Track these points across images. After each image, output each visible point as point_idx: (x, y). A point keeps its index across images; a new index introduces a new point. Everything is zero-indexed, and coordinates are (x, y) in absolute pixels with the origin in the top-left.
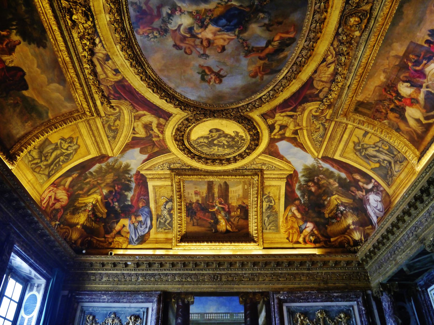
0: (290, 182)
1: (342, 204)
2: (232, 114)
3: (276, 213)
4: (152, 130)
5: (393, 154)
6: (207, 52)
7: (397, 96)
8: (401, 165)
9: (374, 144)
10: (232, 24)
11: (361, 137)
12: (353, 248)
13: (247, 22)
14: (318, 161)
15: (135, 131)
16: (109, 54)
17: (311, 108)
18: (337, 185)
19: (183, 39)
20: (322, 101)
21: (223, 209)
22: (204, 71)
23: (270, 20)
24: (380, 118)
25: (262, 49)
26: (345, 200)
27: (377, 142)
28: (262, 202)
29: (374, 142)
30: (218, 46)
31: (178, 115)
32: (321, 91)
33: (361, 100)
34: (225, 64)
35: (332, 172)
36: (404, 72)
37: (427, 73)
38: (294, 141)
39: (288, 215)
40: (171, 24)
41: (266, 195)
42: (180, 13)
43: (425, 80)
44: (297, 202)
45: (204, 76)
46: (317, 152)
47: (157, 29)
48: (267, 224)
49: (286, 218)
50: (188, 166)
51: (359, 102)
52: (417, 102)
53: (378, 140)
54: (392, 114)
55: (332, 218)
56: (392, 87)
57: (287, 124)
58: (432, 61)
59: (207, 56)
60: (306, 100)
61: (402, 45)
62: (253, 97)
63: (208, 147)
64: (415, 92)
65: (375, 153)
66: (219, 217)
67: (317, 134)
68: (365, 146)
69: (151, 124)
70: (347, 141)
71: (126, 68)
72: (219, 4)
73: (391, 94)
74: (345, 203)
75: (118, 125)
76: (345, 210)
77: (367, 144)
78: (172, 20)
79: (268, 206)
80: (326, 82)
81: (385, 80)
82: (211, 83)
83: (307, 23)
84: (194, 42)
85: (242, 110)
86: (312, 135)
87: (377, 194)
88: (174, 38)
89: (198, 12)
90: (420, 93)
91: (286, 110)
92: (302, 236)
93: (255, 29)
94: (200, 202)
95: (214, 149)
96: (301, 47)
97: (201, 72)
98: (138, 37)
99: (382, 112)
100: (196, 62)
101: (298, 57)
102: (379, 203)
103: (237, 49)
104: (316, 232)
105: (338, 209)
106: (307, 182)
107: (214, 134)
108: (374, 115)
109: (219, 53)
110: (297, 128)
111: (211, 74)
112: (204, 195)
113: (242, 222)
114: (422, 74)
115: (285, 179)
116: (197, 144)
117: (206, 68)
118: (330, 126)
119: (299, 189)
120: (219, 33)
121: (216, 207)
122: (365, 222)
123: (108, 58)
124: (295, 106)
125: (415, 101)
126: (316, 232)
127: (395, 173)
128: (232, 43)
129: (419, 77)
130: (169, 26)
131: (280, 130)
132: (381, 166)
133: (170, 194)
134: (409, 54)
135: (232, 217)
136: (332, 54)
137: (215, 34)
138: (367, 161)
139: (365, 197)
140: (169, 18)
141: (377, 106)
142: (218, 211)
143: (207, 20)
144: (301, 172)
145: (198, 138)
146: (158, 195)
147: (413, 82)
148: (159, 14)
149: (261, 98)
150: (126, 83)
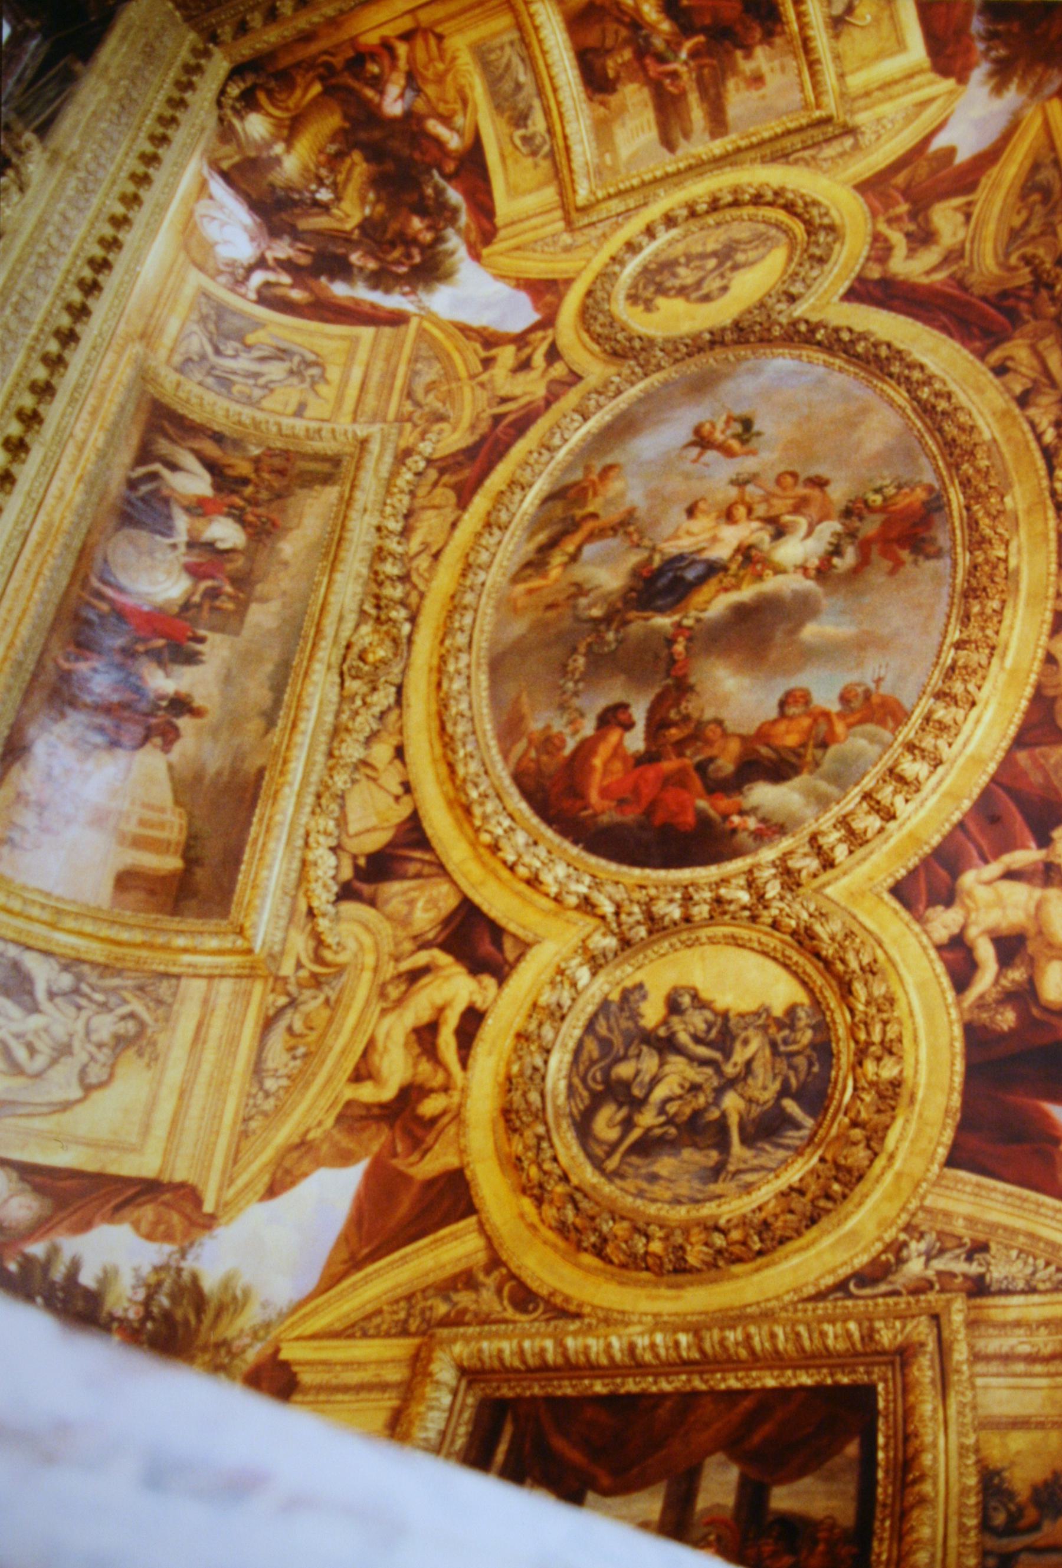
1: (324, 208)
2: (660, 354)
3: (499, 108)
5: (217, 377)
6: (733, 492)
9: (272, 391)
11: (311, 399)
12: (249, 83)
13: (632, 589)
20: (430, 462)
21: (661, 59)
22: (744, 442)
25: (591, 537)
26: (321, 222)
28: (550, 131)
30: (706, 513)
31: (825, 302)
32: (435, 484)
34: (687, 476)
36: (238, 570)
38: (490, 340)
41: (545, 157)
44: (450, 167)
46: (425, 330)
48: (516, 61)
49: (465, 102)
50: (796, 162)
51: (334, 483)
52: (188, 510)
53: (265, 404)
55: (339, 156)
56: (258, 534)
60: (470, 453)
61: (258, 625)
65: (265, 368)
66: (666, 26)
68: (295, 380)
72: (704, 610)
73: (258, 516)
74: (318, 215)
80: (424, 508)
82: (724, 418)
85: (633, 373)
87: (232, 264)
88: (826, 501)
89: (759, 577)
90: (189, 531)
92: (402, 64)
94: (739, 54)
96: (494, 569)
99: (272, 471)
100: (765, 459)
101: (499, 543)
103: (656, 522)
104: (370, 93)
105: (335, 187)
106: (439, 239)
107: (718, 283)
109: (703, 499)
110: (485, 377)
112: (731, 84)
113: (592, 38)
114: (194, 572)
118: (400, 405)
121: (683, 55)
122: (246, 175)
126: (370, 93)
127: (195, 328)
128: (670, 531)
129: (200, 565)
132: (241, 339)
133: (844, 44)
135: (627, 42)
136: (420, 575)
137: (715, 539)
138: (283, 345)
142: (674, 46)
143: (734, 567)
144: (462, 260)
146: (886, 26)
149: (585, 419)
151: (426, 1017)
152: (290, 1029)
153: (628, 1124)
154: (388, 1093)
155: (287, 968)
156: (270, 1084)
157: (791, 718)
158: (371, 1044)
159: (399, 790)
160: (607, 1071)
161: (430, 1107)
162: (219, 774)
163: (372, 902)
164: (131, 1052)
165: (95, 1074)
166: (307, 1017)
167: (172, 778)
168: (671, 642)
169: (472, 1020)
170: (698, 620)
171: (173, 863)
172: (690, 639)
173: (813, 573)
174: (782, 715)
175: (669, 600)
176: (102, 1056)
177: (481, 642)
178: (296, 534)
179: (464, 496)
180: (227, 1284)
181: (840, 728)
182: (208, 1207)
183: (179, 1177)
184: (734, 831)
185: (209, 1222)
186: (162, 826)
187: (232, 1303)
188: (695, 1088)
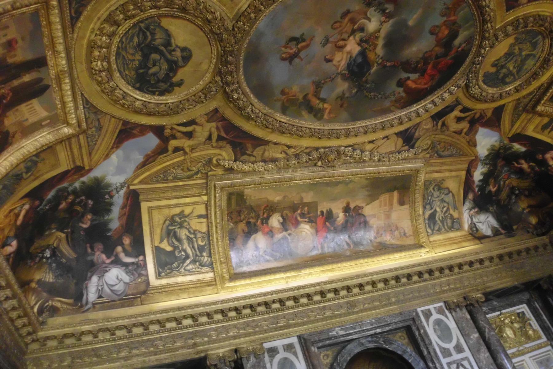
0: (69, 175)
6: (329, 45)
8: (198, 268)
9: (195, 231)
10: (355, 67)
11: (195, 214)
14: (122, 187)
17: (224, 154)
18: (85, 226)
19: (353, 21)
22: (304, 40)
23: (347, 98)
24: (232, 219)
27: (199, 232)
29: (198, 229)
33: (245, 193)
35: (109, 211)
37: (300, 227)
39: (15, 208)
40: (375, 11)
43: (293, 230)
44: (37, 203)
49: (11, 211)
51: (243, 192)
54: (244, 225)
58: (310, 224)
59: (324, 45)
62: (252, 96)
63: (139, 45)
65: (184, 237)
67: (179, 171)
70: (181, 204)
72: (379, 56)
74: (61, 252)
76: (47, 258)
77: (189, 224)
78: (379, 12)
79: (19, 173)
82: (283, 49)
83: (337, 126)
84: (346, 32)
86: (176, 168)
89: (377, 38)
90: (281, 233)
91: (222, 130)
93: (342, 86)
95: (133, 55)
99: (240, 216)
102: (122, 283)
104: (11, 260)
107: (178, 53)
108: (232, 212)
110: (187, 150)
112: (10, 61)
115: (72, 167)
116: (147, 28)
119: (60, 190)
120: (349, 56)
124: (227, 137)
126: (11, 260)
128: (334, 68)
130: (373, 8)
131: (183, 133)
132: (172, 253)
134: (307, 206)
137: (349, 53)
139: (104, 265)
141: (244, 209)
147: (286, 222)
151: (455, 120)
152: (443, 151)
154: (468, 125)
155: (428, 156)
156: (454, 152)
157: (439, 32)
158: (455, 132)
159: (386, 139)
161: (477, 115)
162: (368, 191)
163: (418, 139)
164: (441, 186)
168: (385, 66)
169: (465, 110)
170: (381, 58)
171: (396, 194)
172: (387, 61)
173: (387, 19)
174: (436, 34)
177: (345, 126)
178: (270, 198)
179: (259, 142)
180: (488, 150)
181: (452, 18)
182: (474, 158)
183: (466, 166)
184: (463, 50)
185: (477, 157)
187: (493, 148)
188: (515, 61)
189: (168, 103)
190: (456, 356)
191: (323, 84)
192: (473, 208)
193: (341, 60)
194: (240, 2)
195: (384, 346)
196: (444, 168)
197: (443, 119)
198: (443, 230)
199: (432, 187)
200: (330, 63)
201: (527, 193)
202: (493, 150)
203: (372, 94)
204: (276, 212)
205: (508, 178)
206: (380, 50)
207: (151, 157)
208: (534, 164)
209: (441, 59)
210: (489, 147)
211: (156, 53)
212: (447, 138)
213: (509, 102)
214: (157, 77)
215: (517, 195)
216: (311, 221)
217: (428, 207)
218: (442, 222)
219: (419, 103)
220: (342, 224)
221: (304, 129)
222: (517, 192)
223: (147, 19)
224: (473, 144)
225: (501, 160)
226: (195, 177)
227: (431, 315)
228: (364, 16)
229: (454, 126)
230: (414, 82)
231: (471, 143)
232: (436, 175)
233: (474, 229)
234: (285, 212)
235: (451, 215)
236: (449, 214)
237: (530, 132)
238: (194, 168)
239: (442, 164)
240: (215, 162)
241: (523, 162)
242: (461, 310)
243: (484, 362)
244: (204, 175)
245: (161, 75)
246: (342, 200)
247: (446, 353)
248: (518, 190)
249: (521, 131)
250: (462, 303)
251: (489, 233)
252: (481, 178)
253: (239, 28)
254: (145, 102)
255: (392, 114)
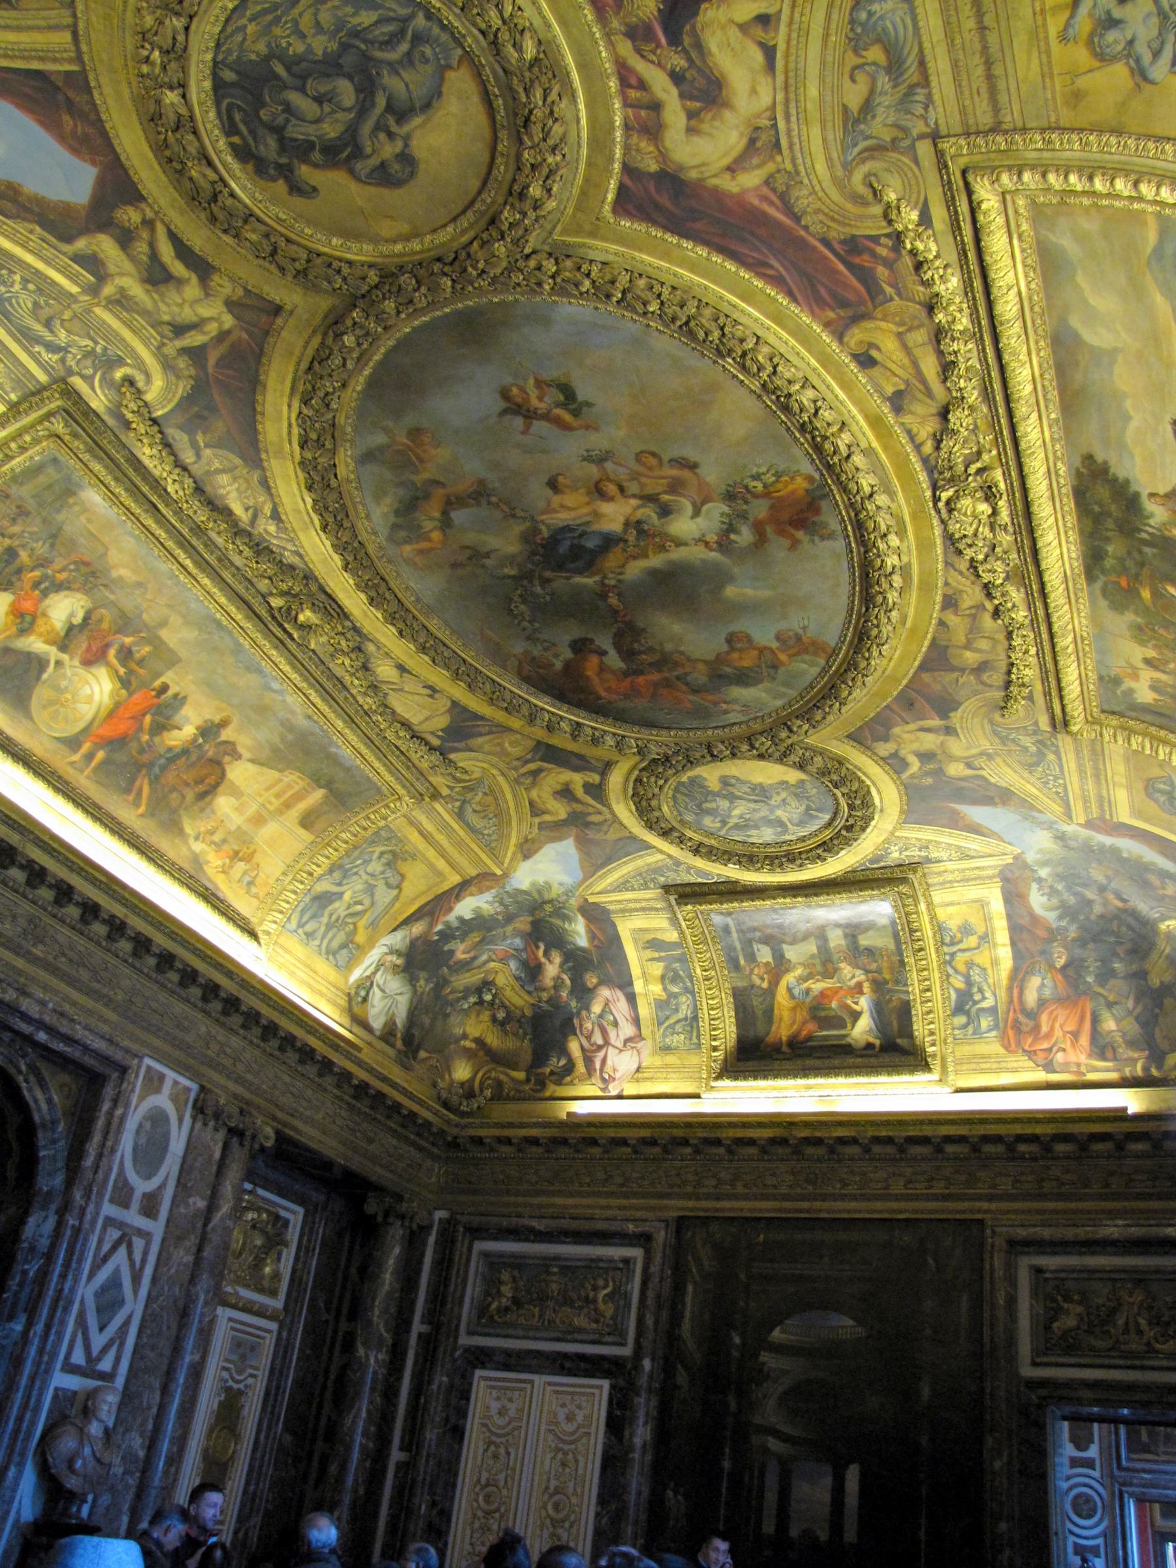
4: (677, 78)
6: (593, 470)
7: (53, 584)
10: (568, 543)
13: (534, 553)
15: (762, 45)
16: (891, 418)
19: (675, 487)
22: (576, 413)
23: (483, 566)
25: (451, 503)
37: (94, 670)
40: (722, 515)
42: (708, 539)
43: (76, 663)
45: (567, 398)
47: (756, 496)
52: (23, 632)
57: (162, 296)
59: (588, 459)
62: (367, 372)
64: (53, 630)
69: (691, 115)
71: (834, 378)
75: (853, 80)
81: (114, 574)
82: (531, 381)
89: (662, 548)
91: (223, 348)
97: (585, 409)
98: (806, 468)
99: (14, 521)
107: (389, 150)
111: (549, 411)
117: (575, 424)
120: (588, 519)
123: (897, 402)
124: (210, 370)
125: (26, 625)
128: (542, 504)
129: (89, 649)
130: (726, 509)
131: (154, 256)
134: (155, 647)
137: (597, 515)
140: (731, 524)
141: (38, 520)
145: (440, 94)
148: (758, 528)
150: (831, 314)
151: (559, 787)
152: (475, 811)
153: (724, 823)
157: (740, 650)
160: (699, 806)
162: (283, 738)
165: (394, 881)
166: (479, 803)
167: (262, 764)
168: (603, 596)
170: (619, 581)
171: (319, 794)
175: (580, 564)
176: (389, 874)
178: (114, 556)
180: (533, 884)
181: (783, 657)
183: (474, 873)
185: (506, 875)
186: (289, 786)
189: (226, 185)
190: (134, 1218)
191: (489, 503)
192: (398, 953)
193: (569, 510)
194: (604, 239)
195: (21, 1078)
196: (441, 838)
197: (546, 765)
198: (317, 942)
199: (383, 849)
200: (549, 492)
201: (501, 1015)
202: (539, 892)
203: (523, 607)
204: (87, 592)
205: (500, 961)
206: (635, 570)
207: (15, 201)
208: (568, 982)
209: (684, 688)
210: (541, 880)
211: (358, 91)
212: (509, 797)
213: (661, 852)
214: (288, 121)
215: (481, 1002)
216: (125, 683)
217: (337, 875)
218: (329, 927)
219: (558, 703)
220: (170, 749)
221: (346, 524)
222: (488, 997)
223: (444, 27)
224: (527, 850)
225: (530, 919)
226: (37, 349)
227: (158, 1090)
228: (699, 501)
229: (544, 792)
230: (602, 669)
231: (526, 847)
232: (414, 836)
233: (363, 993)
234: (103, 611)
235: (355, 931)
236: (354, 924)
237: (626, 928)
238: (63, 334)
239: (445, 827)
240: (118, 374)
241: (557, 959)
242: (216, 1130)
243: (173, 1271)
244: (59, 367)
245: (297, 131)
246: (224, 705)
247: (123, 1196)
248: (494, 996)
249: (616, 912)
250: (229, 1117)
251: (377, 1024)
252: (468, 916)
253: (539, 268)
254: (192, 118)
255: (498, 669)
